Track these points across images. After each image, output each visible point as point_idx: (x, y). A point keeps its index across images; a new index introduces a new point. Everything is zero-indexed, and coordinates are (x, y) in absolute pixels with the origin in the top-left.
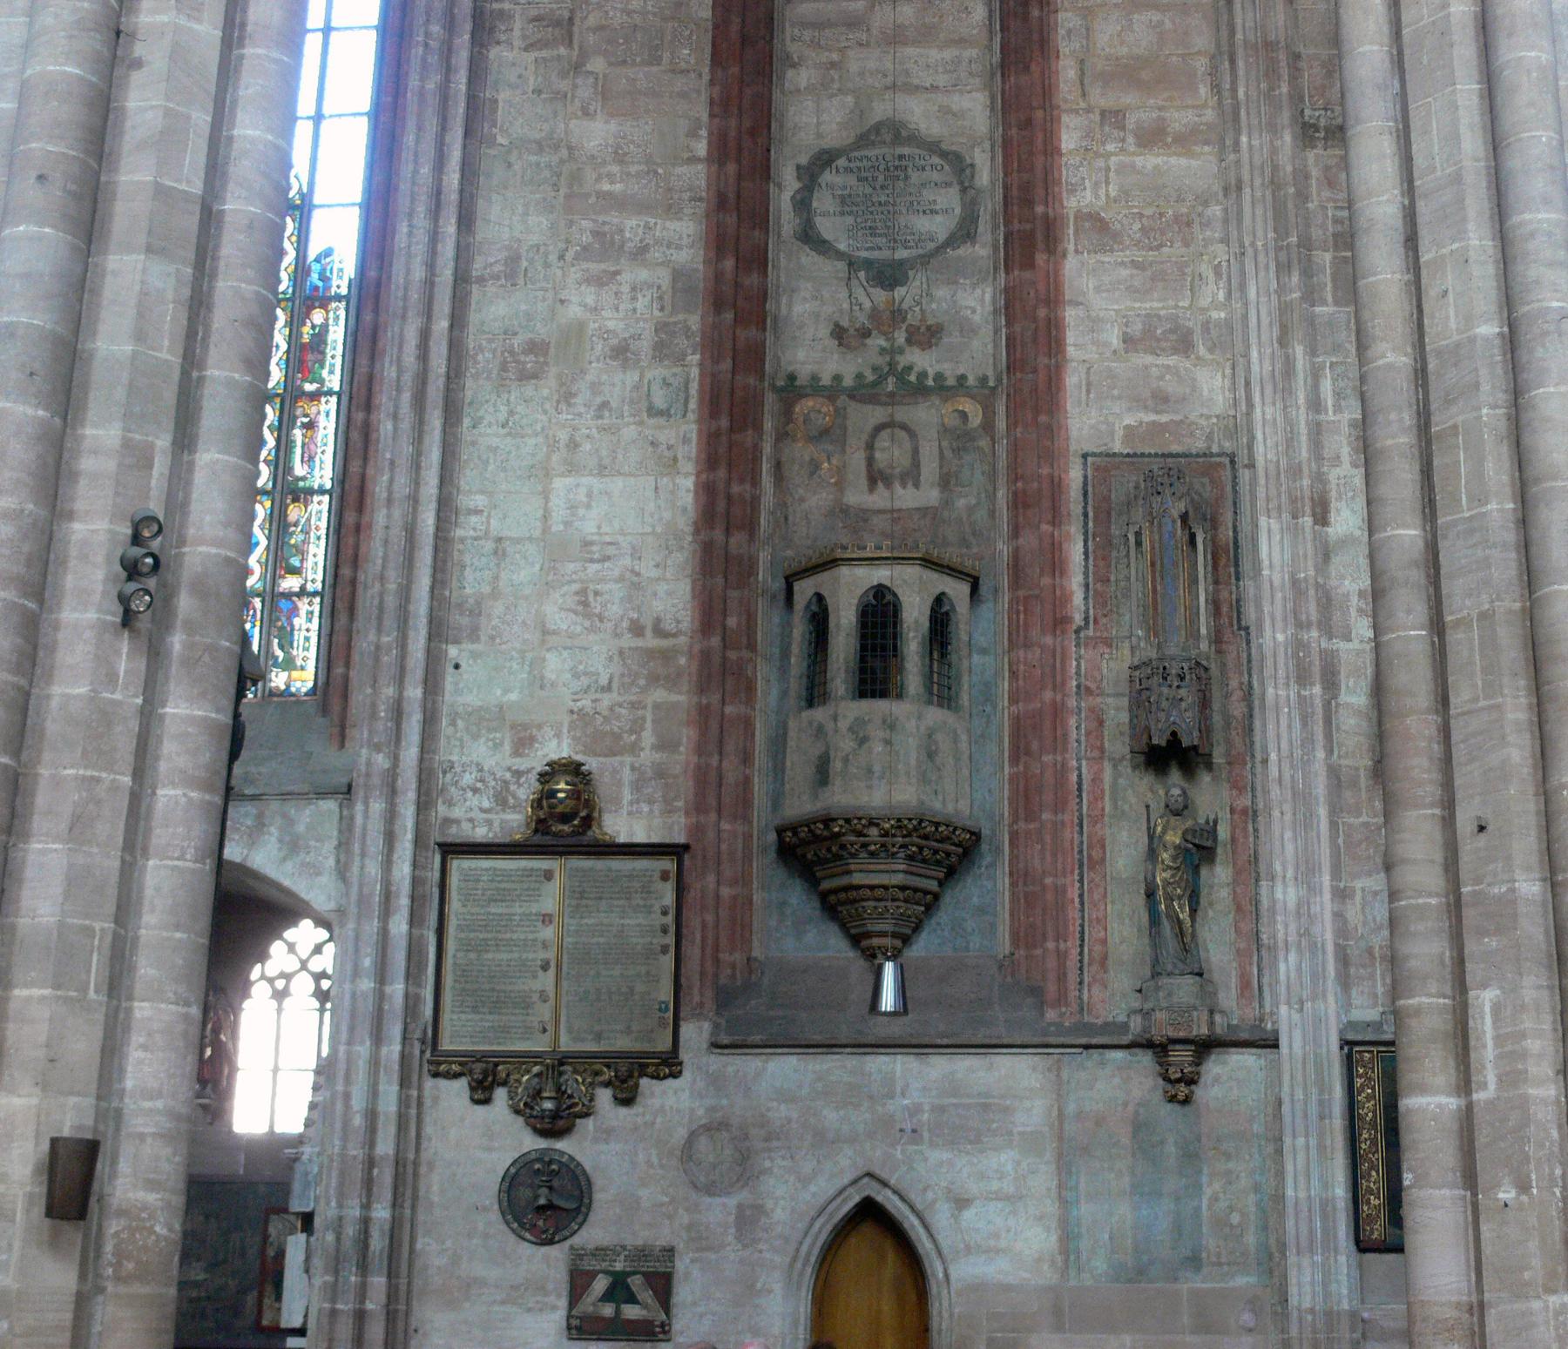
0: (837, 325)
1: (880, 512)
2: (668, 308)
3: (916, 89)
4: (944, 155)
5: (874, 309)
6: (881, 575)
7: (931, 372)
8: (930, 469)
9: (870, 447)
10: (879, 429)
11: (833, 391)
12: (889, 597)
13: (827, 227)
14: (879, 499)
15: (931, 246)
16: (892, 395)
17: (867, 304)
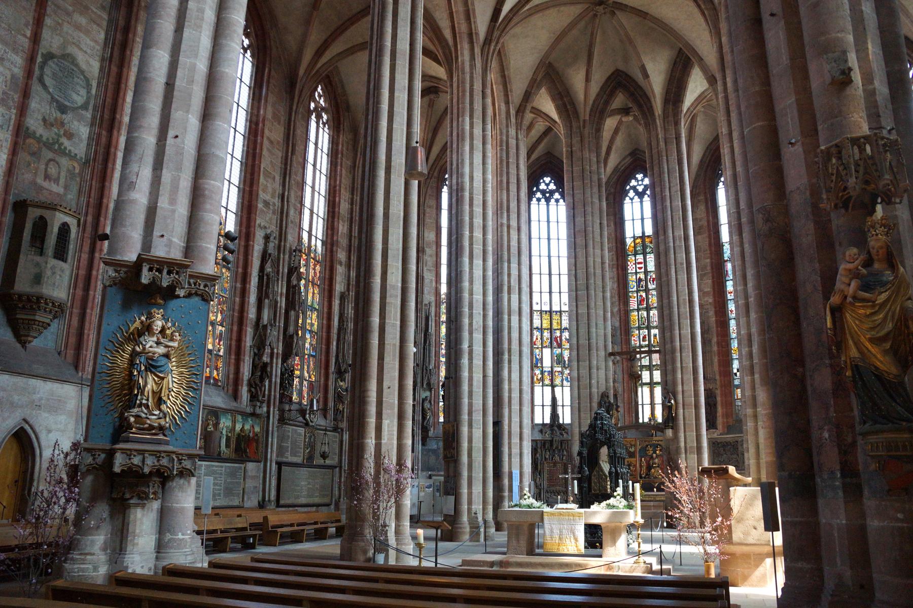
0: (44, 117)
1: (47, 190)
2: (8, 88)
3: (81, 49)
4: (85, 77)
5: (56, 118)
6: (68, 219)
7: (68, 149)
8: (62, 181)
9: (47, 165)
10: (51, 160)
11: (39, 140)
12: (66, 227)
13: (48, 81)
14: (46, 184)
15: (76, 106)
16: (56, 150)
17: (55, 115)
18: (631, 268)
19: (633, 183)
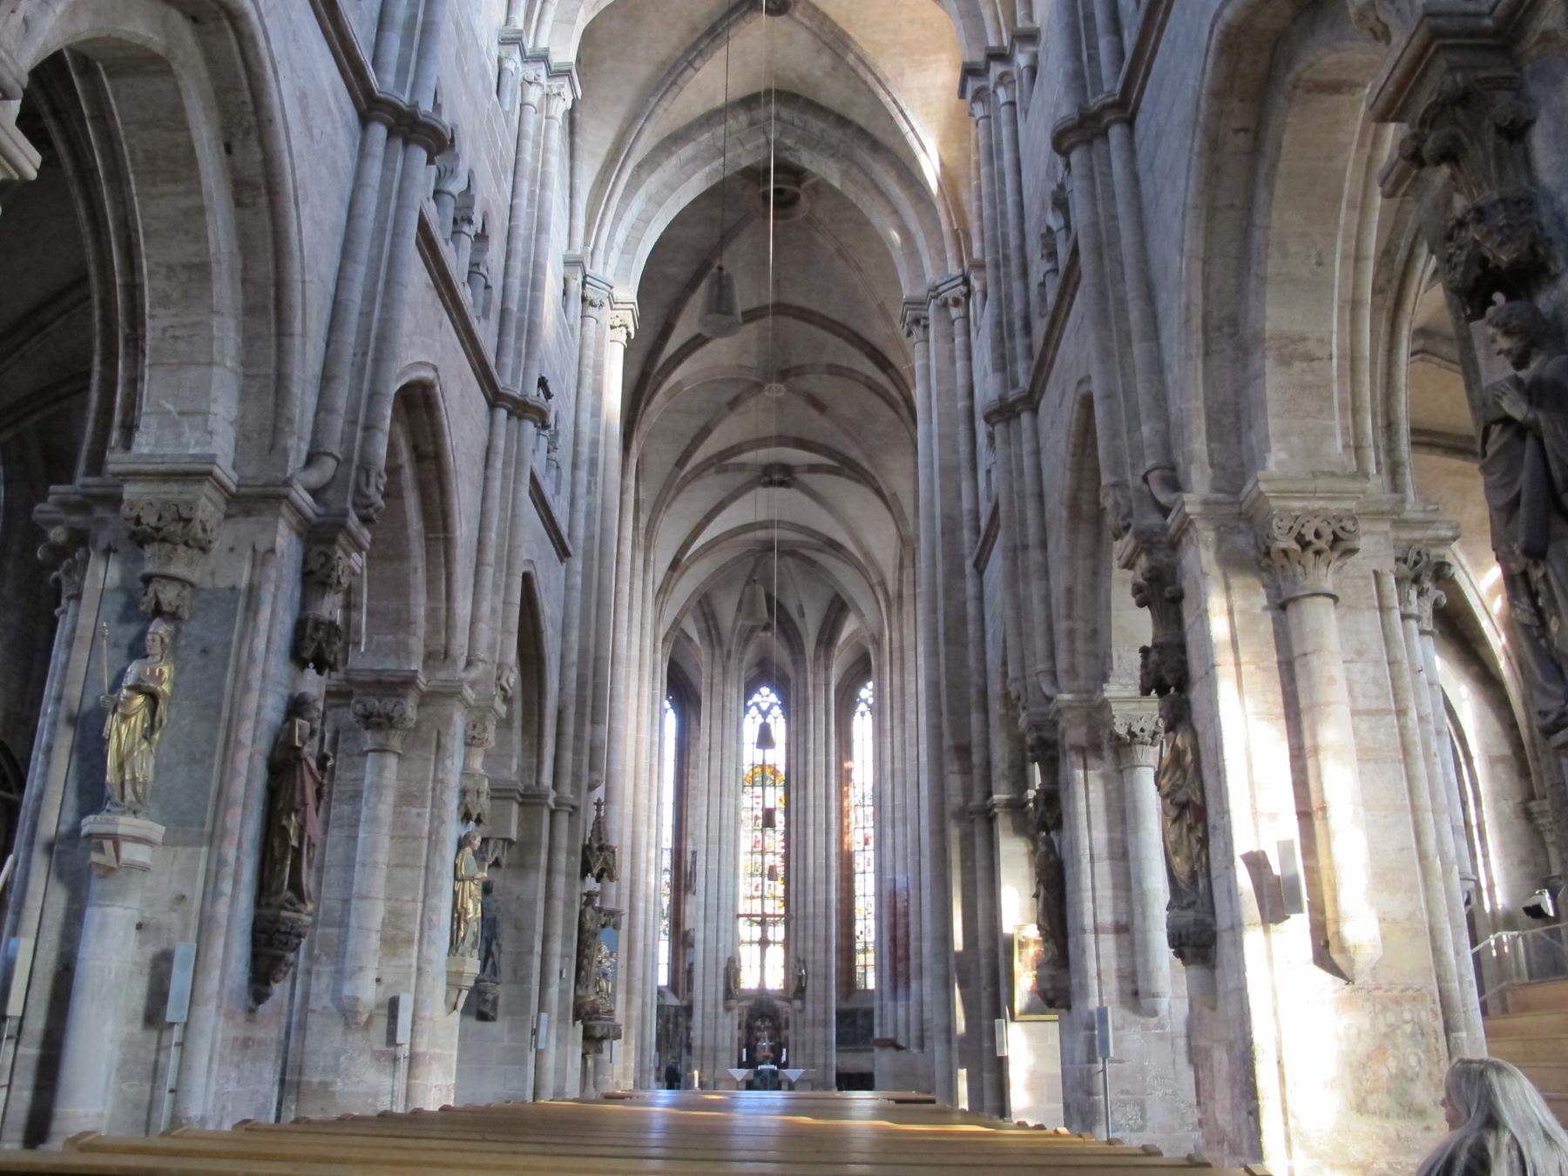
18: (746, 800)
19: (756, 698)
